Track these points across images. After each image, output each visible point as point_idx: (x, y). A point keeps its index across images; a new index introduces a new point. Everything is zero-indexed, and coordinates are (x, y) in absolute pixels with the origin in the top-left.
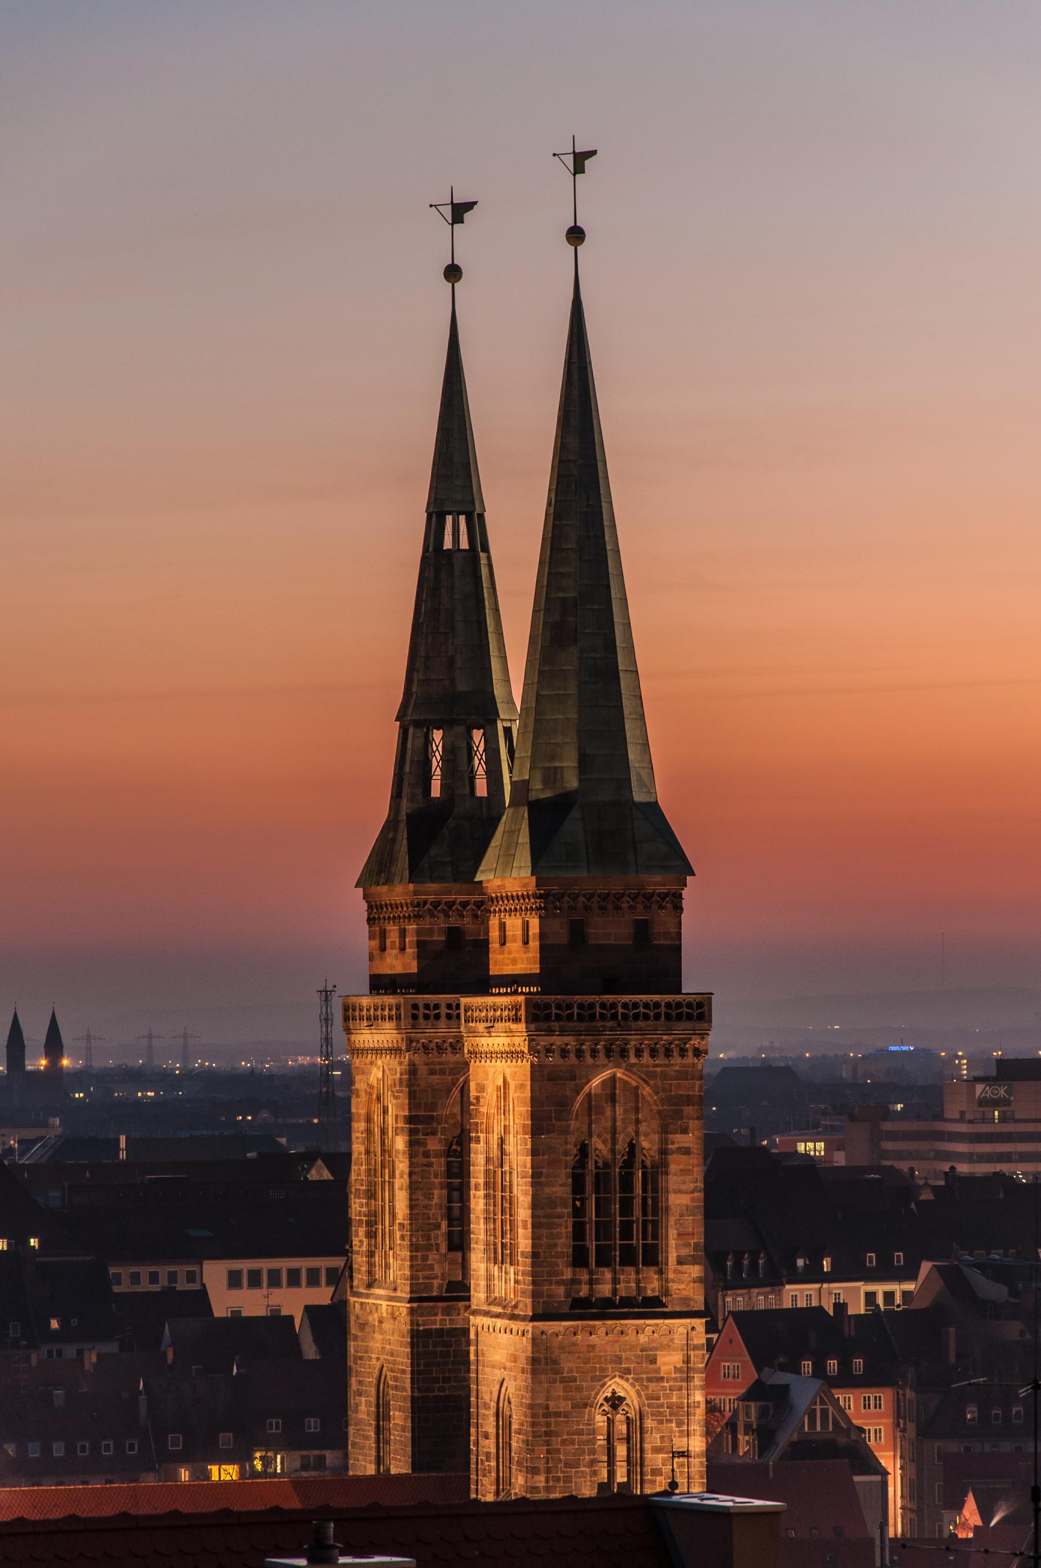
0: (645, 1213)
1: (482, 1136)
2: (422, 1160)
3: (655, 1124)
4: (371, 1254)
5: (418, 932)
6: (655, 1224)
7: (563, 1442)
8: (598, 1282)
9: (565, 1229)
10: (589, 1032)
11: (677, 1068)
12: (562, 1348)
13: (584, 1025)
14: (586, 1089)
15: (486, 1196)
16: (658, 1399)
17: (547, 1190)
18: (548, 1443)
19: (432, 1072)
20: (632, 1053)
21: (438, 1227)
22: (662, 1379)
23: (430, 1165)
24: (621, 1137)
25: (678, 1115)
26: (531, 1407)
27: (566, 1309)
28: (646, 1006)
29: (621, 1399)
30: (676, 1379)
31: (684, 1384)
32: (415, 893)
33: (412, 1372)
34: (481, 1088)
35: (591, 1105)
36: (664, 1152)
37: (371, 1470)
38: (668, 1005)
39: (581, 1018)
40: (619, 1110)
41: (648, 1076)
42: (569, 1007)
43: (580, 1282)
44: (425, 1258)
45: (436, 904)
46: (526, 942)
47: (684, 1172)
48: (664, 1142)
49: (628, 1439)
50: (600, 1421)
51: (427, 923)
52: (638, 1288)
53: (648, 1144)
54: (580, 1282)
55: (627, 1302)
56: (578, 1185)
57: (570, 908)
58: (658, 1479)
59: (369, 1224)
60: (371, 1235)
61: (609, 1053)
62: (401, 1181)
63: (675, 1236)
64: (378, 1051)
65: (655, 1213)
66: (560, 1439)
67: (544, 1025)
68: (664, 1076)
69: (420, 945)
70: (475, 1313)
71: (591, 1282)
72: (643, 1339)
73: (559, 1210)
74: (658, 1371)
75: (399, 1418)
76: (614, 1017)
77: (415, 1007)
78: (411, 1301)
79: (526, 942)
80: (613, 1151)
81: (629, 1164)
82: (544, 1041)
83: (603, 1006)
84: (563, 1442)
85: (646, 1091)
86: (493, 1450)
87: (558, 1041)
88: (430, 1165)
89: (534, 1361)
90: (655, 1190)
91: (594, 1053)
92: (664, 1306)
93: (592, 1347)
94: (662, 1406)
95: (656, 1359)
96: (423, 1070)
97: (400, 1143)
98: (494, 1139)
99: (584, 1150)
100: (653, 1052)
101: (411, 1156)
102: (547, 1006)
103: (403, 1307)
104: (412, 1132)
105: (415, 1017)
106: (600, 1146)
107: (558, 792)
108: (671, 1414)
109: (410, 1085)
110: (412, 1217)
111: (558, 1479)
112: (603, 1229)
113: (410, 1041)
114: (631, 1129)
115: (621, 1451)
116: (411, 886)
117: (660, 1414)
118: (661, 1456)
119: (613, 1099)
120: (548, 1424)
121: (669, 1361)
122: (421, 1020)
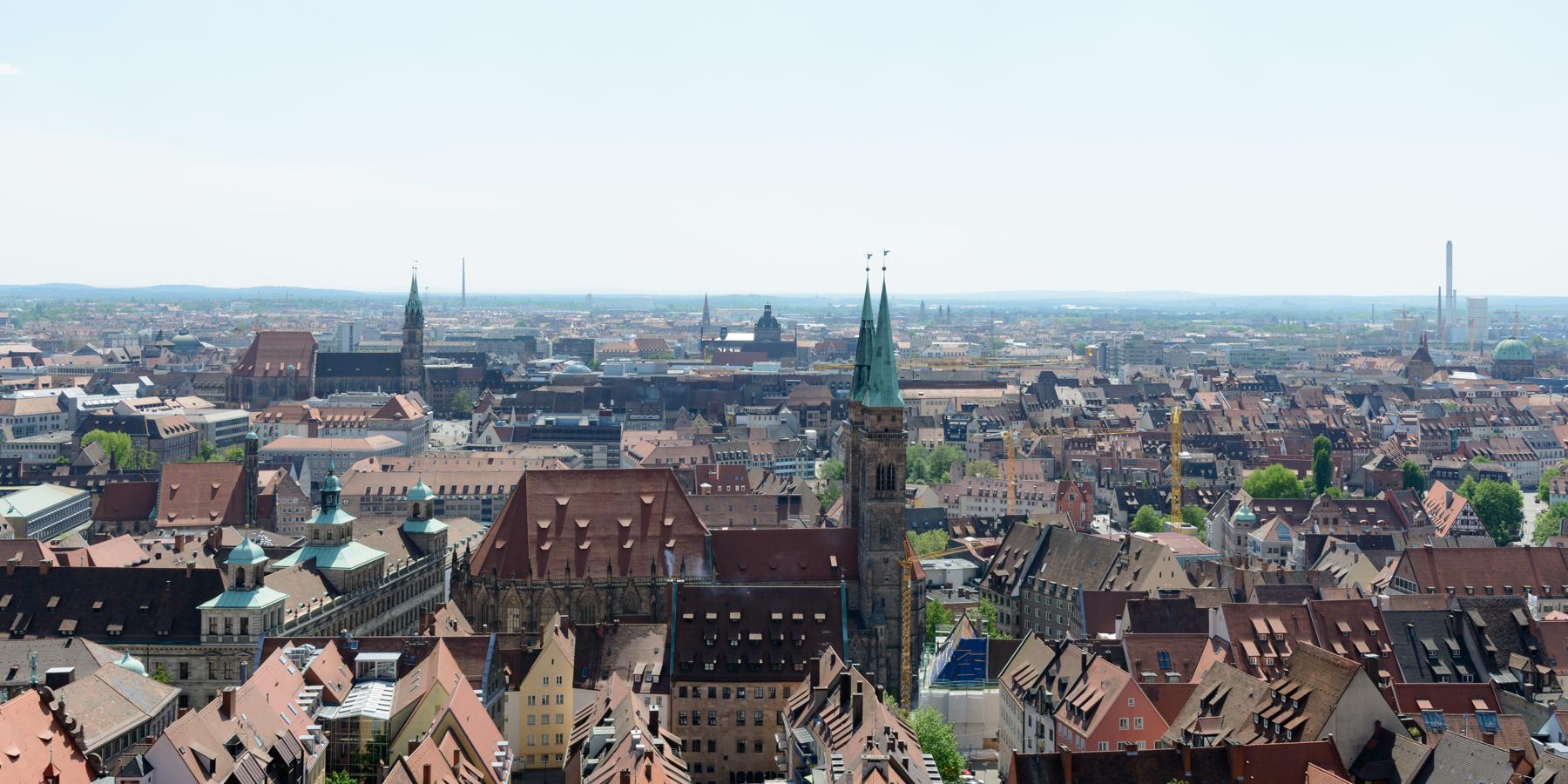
56: (878, 472)
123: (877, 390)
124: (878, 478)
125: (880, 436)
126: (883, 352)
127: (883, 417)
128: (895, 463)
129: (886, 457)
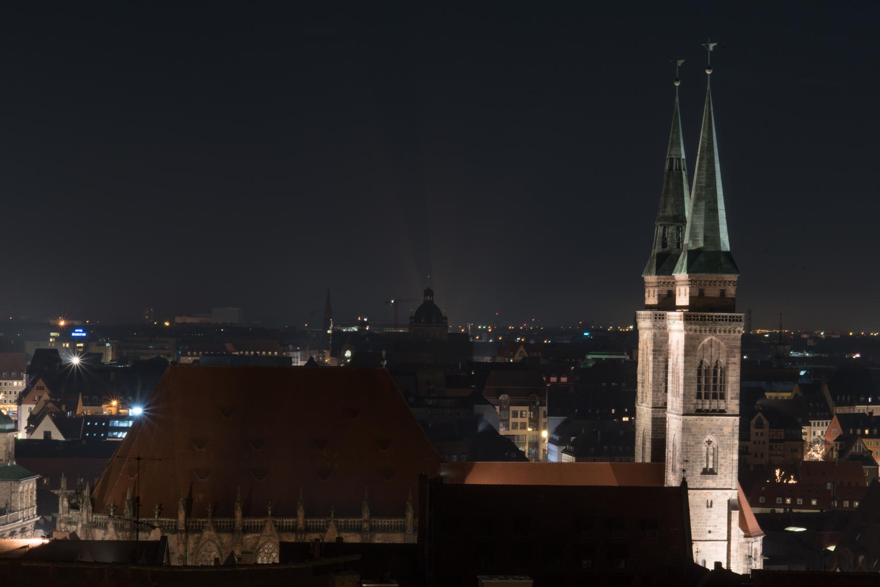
0: (721, 383)
1: (672, 356)
2: (657, 364)
3: (725, 354)
4: (643, 393)
5: (658, 291)
6: (724, 386)
7: (692, 455)
8: (705, 404)
9: (695, 387)
10: (704, 324)
11: (732, 337)
12: (692, 424)
13: (702, 322)
14: (703, 342)
15: (672, 376)
17: (689, 374)
18: (687, 455)
19: (661, 336)
20: (718, 332)
21: (661, 385)
22: (724, 436)
23: (659, 365)
24: (713, 358)
25: (733, 352)
26: (682, 443)
27: (694, 413)
28: (723, 317)
29: (711, 442)
30: (729, 436)
31: (732, 438)
32: (658, 279)
33: (652, 431)
34: (672, 342)
35: (704, 348)
36: (727, 363)
37: (640, 461)
38: (730, 317)
39: (701, 320)
40: (713, 350)
41: (723, 339)
42: (698, 316)
43: (699, 404)
44: (657, 395)
45: (664, 283)
46: (685, 295)
47: (734, 370)
48: (728, 360)
49: (713, 454)
50: (704, 448)
51: (661, 288)
52: (718, 406)
53: (722, 361)
54: (699, 404)
55: (714, 411)
56: (699, 373)
57: (699, 285)
58: (722, 467)
59: (643, 383)
60: (643, 387)
61: (710, 331)
62: (651, 370)
64: (646, 329)
65: (724, 383)
67: (689, 322)
68: (728, 339)
69: (659, 295)
70: (668, 412)
71: (702, 404)
72: (719, 423)
73: (693, 381)
74: (723, 433)
75: (648, 445)
76: (712, 320)
77: (656, 315)
78: (652, 408)
79: (685, 295)
80: (711, 362)
81: (716, 367)
82: (689, 327)
83: (709, 316)
84: (692, 455)
85: (722, 344)
86: (672, 456)
87: (694, 327)
88: (659, 365)
89: (683, 429)
90: (724, 376)
91: (705, 331)
92: (726, 412)
93: (702, 425)
94: (724, 444)
96: (658, 335)
97: (651, 358)
98: (675, 358)
99: (702, 362)
100: (725, 331)
101: (654, 362)
102: (690, 316)
103: (650, 410)
104: (654, 355)
105: (656, 318)
106: (707, 361)
107: (697, 247)
108: (727, 447)
109: (654, 340)
110: (653, 382)
111: (690, 466)
112: (707, 388)
113: (654, 326)
114: (717, 356)
115: (711, 458)
116: (656, 276)
117: (724, 447)
119: (711, 346)
120: (687, 449)
121: (727, 430)
122: (658, 319)
124: (699, 381)
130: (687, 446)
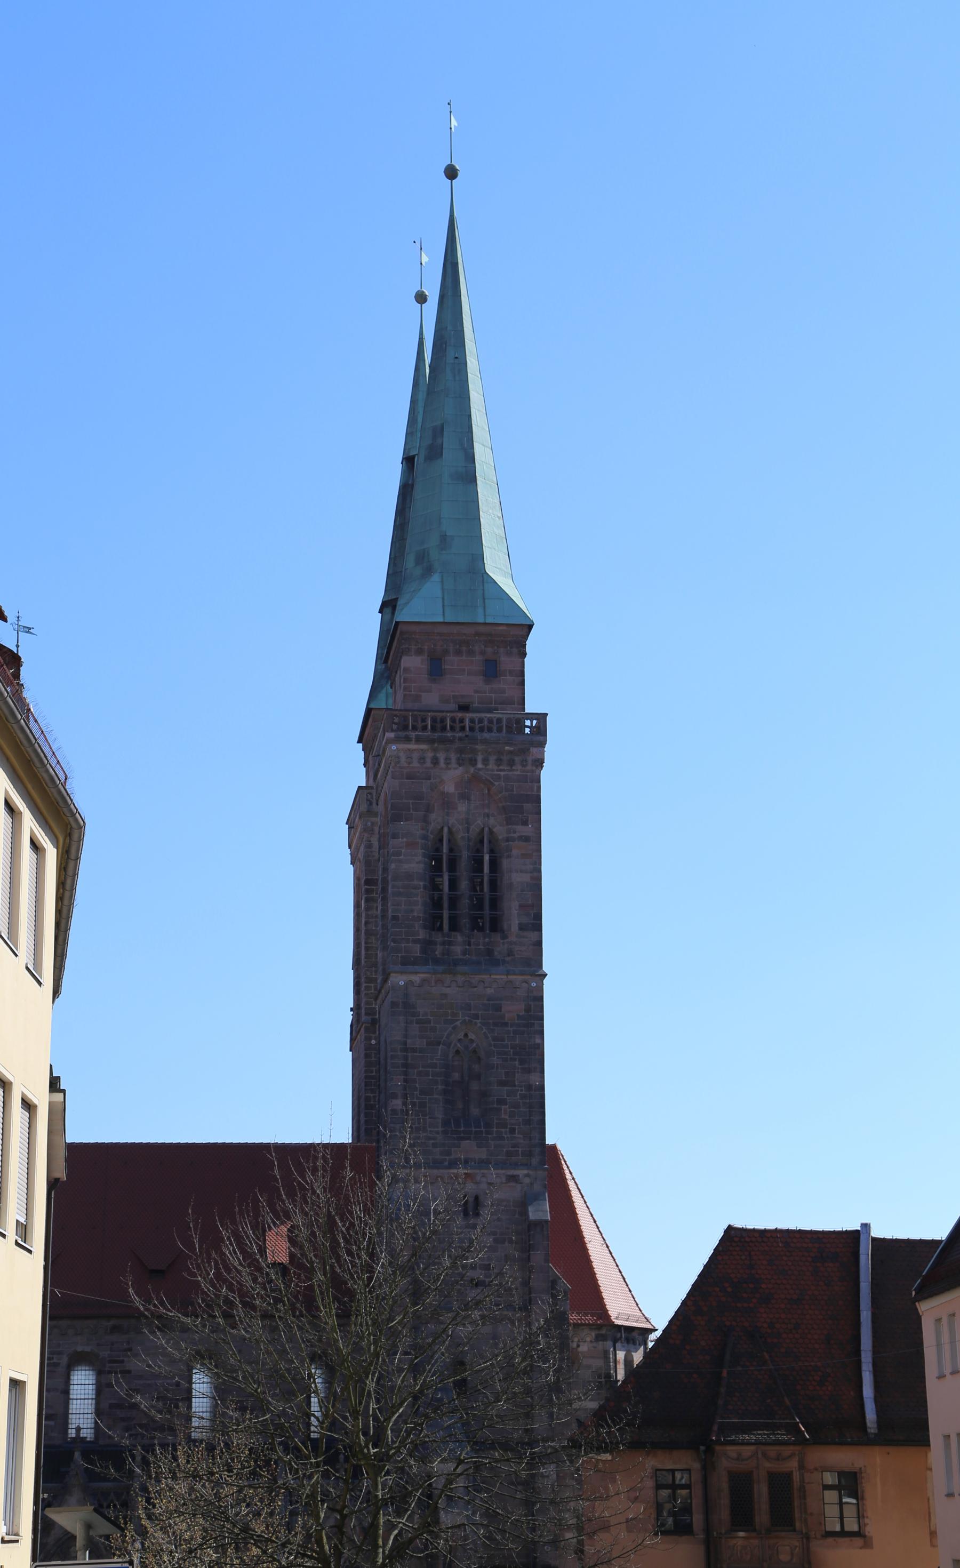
11: (518, 773)
16: (503, 1040)
22: (506, 1024)
43: (435, 944)
54: (435, 944)
58: (503, 1107)
63: (517, 908)
66: (416, 1071)
95: (501, 1007)
118: (505, 1088)
120: (406, 1058)
123: (429, 571)
125: (439, 725)
126: (449, 442)
127: (452, 662)
128: (501, 831)
129: (462, 807)
130: (406, 1050)
